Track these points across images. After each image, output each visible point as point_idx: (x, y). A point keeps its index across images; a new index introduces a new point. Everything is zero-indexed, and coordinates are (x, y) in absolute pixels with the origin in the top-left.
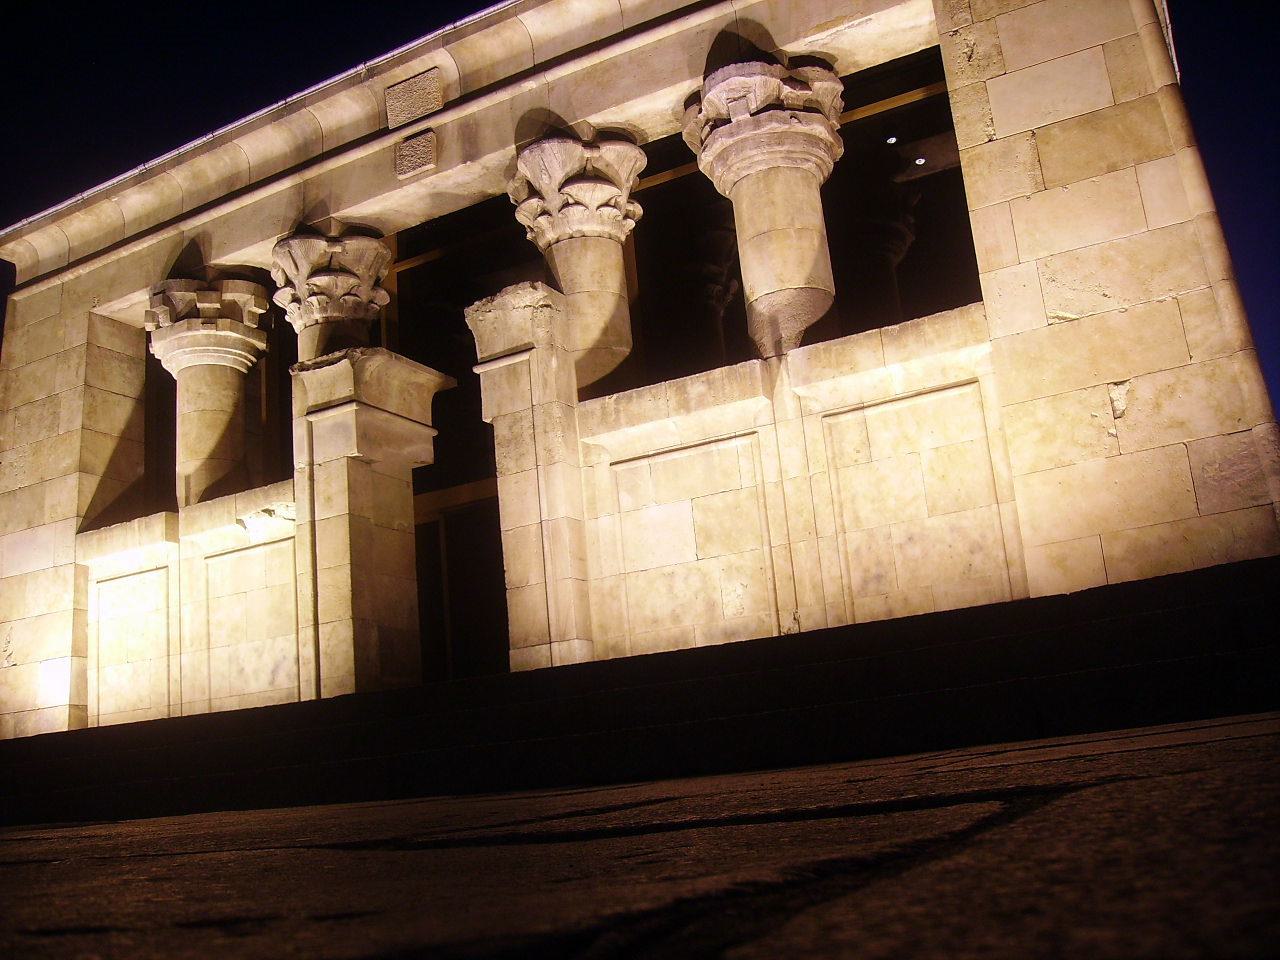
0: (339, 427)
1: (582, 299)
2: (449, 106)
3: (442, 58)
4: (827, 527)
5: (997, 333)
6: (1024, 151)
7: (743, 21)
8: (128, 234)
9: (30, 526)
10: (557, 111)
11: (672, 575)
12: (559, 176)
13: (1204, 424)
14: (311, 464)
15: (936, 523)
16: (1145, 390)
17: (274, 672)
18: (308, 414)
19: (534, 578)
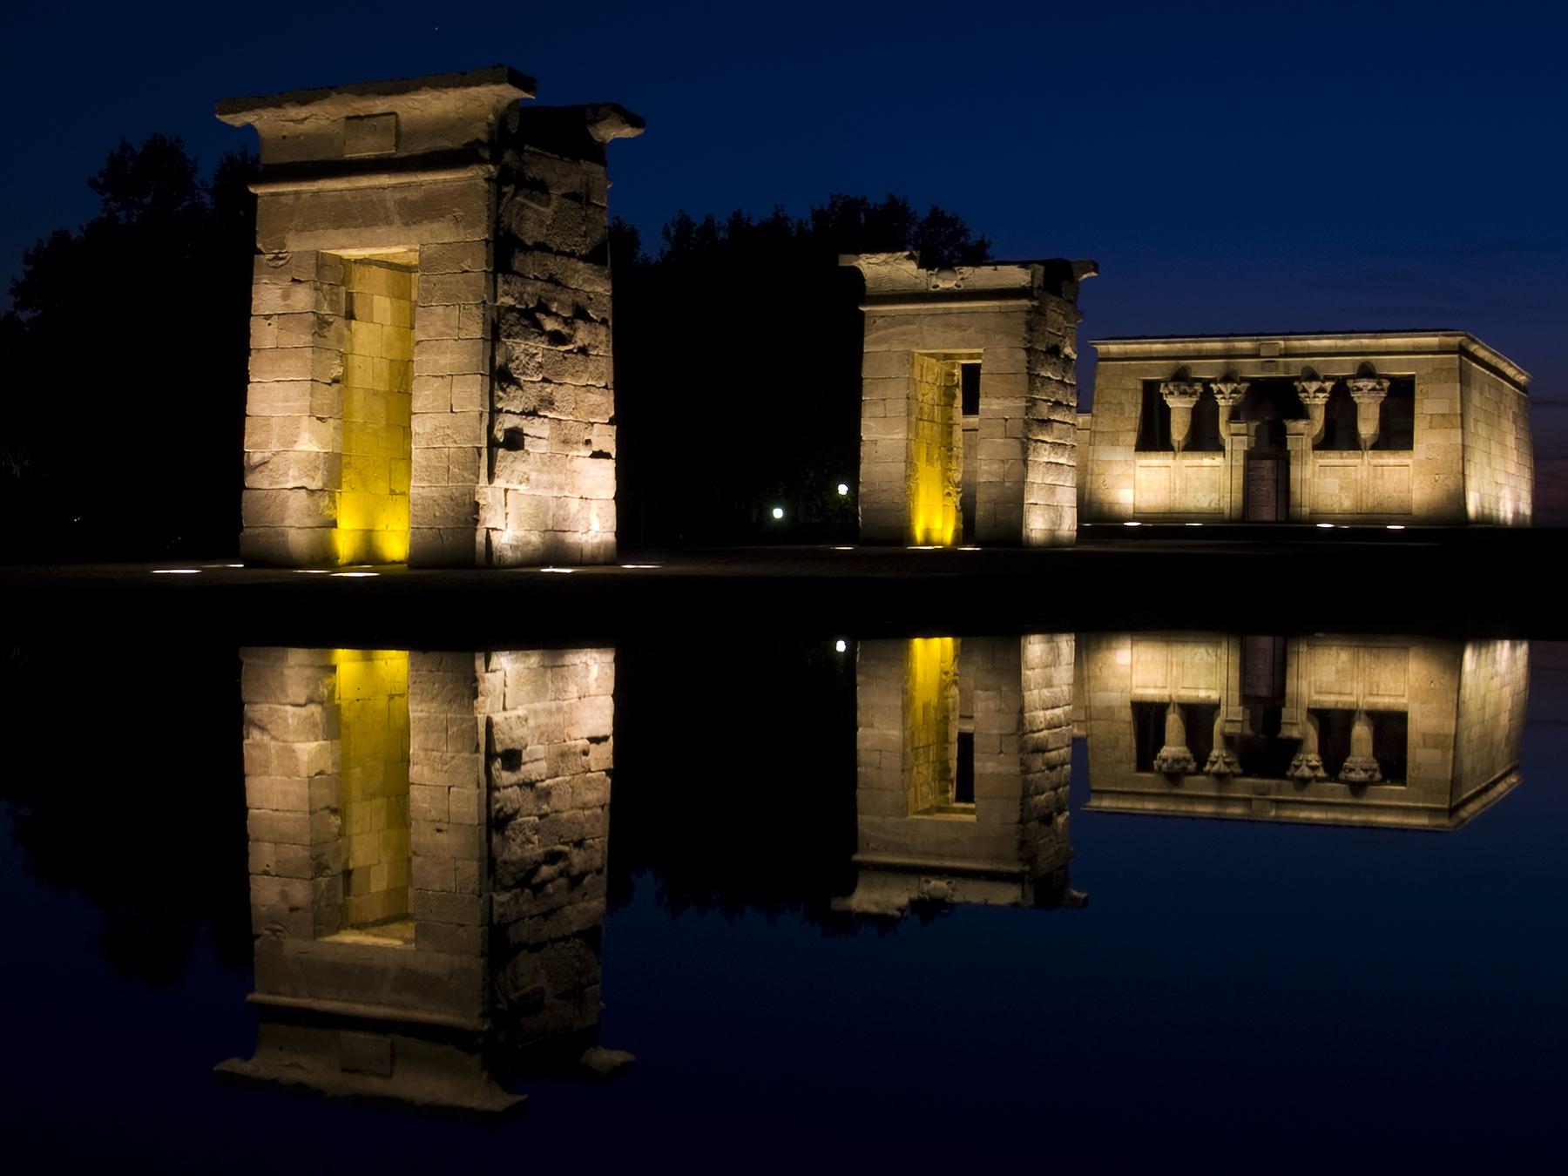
0: (1241, 441)
1: (1315, 422)
2: (1281, 356)
3: (1282, 343)
4: (1371, 491)
5: (1415, 458)
6: (1429, 417)
7: (1368, 362)
8: (1153, 355)
9: (1113, 445)
10: (1315, 369)
11: (1332, 495)
12: (1314, 389)
13: (1452, 487)
14: (1232, 450)
15: (1395, 495)
16: (1442, 477)
17: (1211, 502)
18: (1232, 435)
19: (1299, 491)
